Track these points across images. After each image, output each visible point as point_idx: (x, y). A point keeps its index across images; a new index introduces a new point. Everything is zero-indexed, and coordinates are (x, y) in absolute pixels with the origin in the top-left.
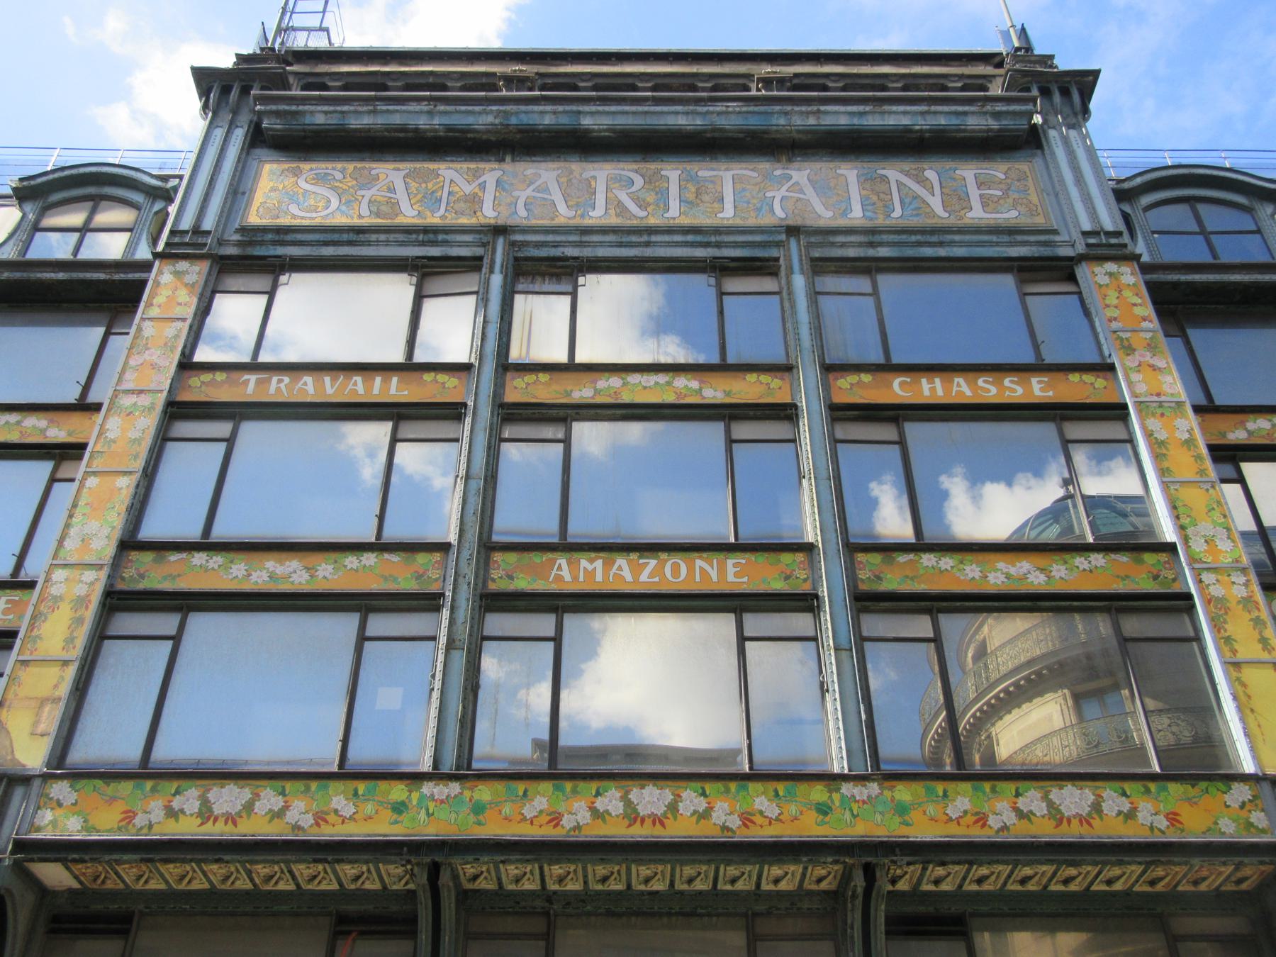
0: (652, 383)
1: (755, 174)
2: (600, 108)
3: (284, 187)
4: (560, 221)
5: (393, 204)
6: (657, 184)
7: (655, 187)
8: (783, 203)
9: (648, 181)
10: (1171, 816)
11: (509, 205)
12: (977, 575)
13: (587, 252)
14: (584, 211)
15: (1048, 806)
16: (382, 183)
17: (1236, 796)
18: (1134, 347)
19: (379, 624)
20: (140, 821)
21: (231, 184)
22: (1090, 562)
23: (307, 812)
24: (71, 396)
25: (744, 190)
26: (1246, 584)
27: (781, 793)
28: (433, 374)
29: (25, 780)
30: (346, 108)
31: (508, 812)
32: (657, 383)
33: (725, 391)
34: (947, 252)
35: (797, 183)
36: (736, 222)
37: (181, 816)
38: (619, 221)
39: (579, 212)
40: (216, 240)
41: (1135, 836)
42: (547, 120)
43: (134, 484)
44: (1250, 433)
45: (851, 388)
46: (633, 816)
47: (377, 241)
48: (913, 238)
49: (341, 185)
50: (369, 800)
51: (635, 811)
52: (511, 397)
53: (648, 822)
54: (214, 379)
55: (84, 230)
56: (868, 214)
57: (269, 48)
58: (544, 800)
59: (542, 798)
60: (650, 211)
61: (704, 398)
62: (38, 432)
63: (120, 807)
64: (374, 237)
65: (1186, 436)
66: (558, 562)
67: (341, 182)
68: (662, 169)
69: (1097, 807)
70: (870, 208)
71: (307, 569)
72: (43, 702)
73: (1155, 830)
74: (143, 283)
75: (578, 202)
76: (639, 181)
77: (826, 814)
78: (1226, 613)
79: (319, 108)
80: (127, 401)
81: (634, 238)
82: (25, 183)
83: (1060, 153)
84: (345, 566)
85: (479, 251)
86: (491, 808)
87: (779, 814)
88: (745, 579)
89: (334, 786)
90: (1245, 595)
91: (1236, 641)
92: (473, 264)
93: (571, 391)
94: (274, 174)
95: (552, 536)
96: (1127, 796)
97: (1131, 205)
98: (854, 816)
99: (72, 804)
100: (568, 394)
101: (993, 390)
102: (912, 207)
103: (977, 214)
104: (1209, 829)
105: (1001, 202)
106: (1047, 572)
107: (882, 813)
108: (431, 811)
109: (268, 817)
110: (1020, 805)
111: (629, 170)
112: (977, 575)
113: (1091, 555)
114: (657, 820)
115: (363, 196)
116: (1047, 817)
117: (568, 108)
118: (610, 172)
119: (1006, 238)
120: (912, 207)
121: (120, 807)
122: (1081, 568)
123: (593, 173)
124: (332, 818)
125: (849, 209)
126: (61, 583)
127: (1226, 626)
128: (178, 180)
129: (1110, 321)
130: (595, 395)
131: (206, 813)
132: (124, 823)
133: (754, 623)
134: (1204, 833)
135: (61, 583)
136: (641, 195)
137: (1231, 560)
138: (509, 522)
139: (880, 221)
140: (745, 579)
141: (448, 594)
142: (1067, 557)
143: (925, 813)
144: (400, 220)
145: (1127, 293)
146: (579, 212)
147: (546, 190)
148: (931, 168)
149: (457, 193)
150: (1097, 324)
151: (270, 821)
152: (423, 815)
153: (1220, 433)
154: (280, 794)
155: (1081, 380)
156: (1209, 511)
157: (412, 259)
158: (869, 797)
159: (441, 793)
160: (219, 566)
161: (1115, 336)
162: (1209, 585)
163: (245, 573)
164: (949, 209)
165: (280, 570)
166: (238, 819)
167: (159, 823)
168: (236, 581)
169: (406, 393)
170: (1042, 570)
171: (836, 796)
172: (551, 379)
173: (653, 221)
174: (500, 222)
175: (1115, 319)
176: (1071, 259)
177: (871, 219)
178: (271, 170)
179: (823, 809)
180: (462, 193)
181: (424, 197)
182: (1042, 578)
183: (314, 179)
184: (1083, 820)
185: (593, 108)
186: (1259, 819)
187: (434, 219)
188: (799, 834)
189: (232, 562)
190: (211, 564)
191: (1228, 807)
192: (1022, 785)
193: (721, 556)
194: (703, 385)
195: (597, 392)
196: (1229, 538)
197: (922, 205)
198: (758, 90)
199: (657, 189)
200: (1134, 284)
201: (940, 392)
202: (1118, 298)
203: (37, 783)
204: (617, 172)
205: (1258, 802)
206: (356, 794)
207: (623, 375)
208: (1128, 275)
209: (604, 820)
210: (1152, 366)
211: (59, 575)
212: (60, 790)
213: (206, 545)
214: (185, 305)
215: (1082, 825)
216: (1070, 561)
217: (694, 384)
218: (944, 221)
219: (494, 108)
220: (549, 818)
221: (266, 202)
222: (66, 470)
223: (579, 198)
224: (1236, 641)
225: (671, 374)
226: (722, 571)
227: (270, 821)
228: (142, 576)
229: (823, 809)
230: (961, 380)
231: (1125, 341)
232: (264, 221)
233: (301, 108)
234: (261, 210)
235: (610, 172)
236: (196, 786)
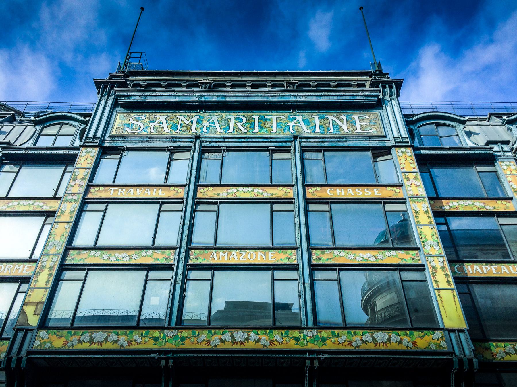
0: (247, 191)
1: (284, 117)
2: (232, 94)
4: (218, 134)
5: (162, 128)
8: (293, 127)
9: (248, 120)
10: (414, 343)
11: (201, 128)
12: (352, 258)
13: (227, 145)
15: (372, 339)
17: (436, 336)
18: (410, 178)
19: (153, 275)
20: (69, 344)
21: (107, 121)
22: (391, 254)
23: (125, 341)
24: (51, 195)
25: (280, 123)
26: (443, 262)
27: (283, 334)
28: (173, 188)
29: (32, 330)
30: (146, 94)
31: (192, 340)
32: (248, 191)
33: (271, 194)
34: (348, 144)
35: (298, 120)
37: (83, 343)
39: (224, 131)
40: (101, 141)
41: (401, 350)
42: (215, 99)
43: (71, 227)
44: (450, 207)
45: (313, 193)
46: (234, 341)
47: (156, 141)
48: (337, 140)
49: (144, 121)
50: (146, 336)
51: (235, 340)
52: (199, 195)
53: (239, 343)
54: (99, 190)
55: (57, 135)
56: (322, 131)
57: (121, 71)
58: (205, 336)
59: (204, 335)
61: (264, 196)
62: (40, 207)
63: (63, 339)
64: (155, 140)
65: (426, 210)
66: (213, 253)
67: (144, 120)
68: (253, 116)
69: (389, 340)
70: (322, 129)
72: (38, 303)
73: (409, 348)
74: (76, 155)
76: (245, 120)
77: (298, 341)
78: (436, 272)
79: (137, 94)
80: (70, 197)
81: (242, 140)
82: (37, 119)
83: (389, 108)
84: (142, 255)
85: (190, 144)
86: (187, 339)
87: (283, 341)
88: (275, 259)
89: (135, 332)
90: (443, 266)
91: (439, 282)
92: (187, 149)
93: (220, 193)
94: (122, 117)
95: (212, 244)
96: (400, 336)
97: (414, 126)
98: (308, 342)
99: (47, 339)
100: (218, 194)
101: (361, 193)
102: (336, 129)
103: (359, 131)
104: (426, 347)
106: (376, 257)
107: (317, 341)
108: (167, 340)
109: (112, 343)
110: (363, 338)
111: (241, 116)
112: (352, 258)
113: (391, 251)
114: (242, 343)
116: (372, 343)
117: (222, 94)
118: (235, 116)
119: (368, 140)
120: (336, 129)
121: (63, 339)
122: (388, 256)
123: (229, 117)
124: (134, 343)
125: (315, 129)
126: (45, 262)
127: (436, 276)
128: (89, 118)
129: (402, 169)
130: (227, 195)
131: (91, 342)
132: (64, 345)
133: (278, 274)
134: (425, 349)
135: (45, 262)
136: (245, 124)
137: (438, 253)
138: (197, 239)
139: (326, 134)
140: (275, 259)
141: (176, 264)
142: (383, 251)
143: (331, 341)
144: (164, 134)
145: (409, 159)
146: (224, 131)
147: (213, 123)
149: (183, 124)
150: (398, 170)
151: (113, 344)
152: (164, 342)
153: (440, 207)
154: (117, 335)
156: (432, 236)
157: (168, 148)
158: (313, 335)
159: (170, 334)
160: (99, 255)
161: (403, 174)
162: (431, 262)
163: (108, 258)
164: (349, 129)
165: (120, 257)
166: (102, 344)
167: (76, 345)
168: (105, 260)
169: (164, 194)
170: (375, 256)
171: (302, 335)
172: (213, 189)
173: (249, 134)
174: (198, 134)
175: (404, 168)
176: (390, 147)
177: (322, 133)
178: (121, 116)
182: (374, 259)
184: (385, 344)
185: (230, 94)
186: (443, 344)
187: (175, 134)
188: (289, 348)
189: (103, 254)
190: (97, 255)
191: (433, 340)
192: (364, 331)
193: (267, 251)
194: (264, 192)
195: (228, 194)
196: (438, 246)
198: (287, 87)
199: (251, 123)
200: (411, 156)
201: (343, 194)
203: (36, 331)
204: (238, 116)
205: (444, 338)
206: (142, 335)
207: (237, 188)
208: (409, 152)
209: (224, 343)
210: (416, 185)
211: (44, 258)
212: (43, 333)
213: (95, 248)
214: (90, 163)
215: (384, 346)
216: (384, 253)
217: (261, 191)
219: (197, 94)
220: (206, 342)
222: (50, 220)
223: (224, 126)
224: (439, 282)
225: (253, 187)
226: (267, 256)
227: (113, 344)
228: (73, 259)
229: (297, 339)
230: (350, 190)
233: (131, 94)
234: (117, 129)
235: (235, 116)
236: (89, 332)
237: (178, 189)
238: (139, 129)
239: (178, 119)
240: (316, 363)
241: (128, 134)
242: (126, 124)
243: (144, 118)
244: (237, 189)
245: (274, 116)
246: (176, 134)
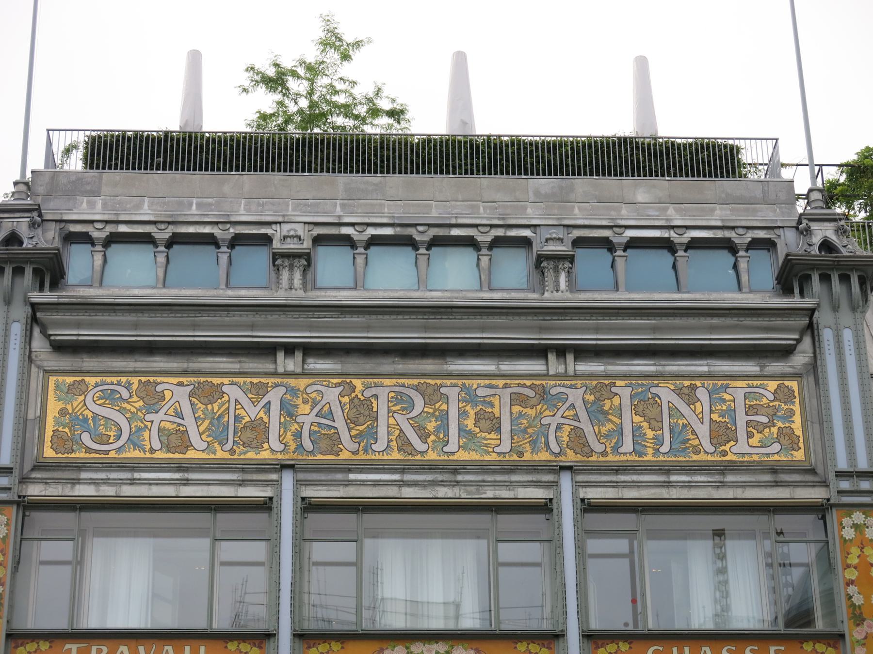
1: (531, 393)
3: (73, 410)
4: (345, 455)
6: (437, 405)
7: (435, 410)
14: (367, 443)
16: (167, 407)
36: (512, 459)
38: (402, 458)
49: (128, 407)
56: (637, 447)
60: (430, 444)
67: (128, 403)
68: (441, 386)
75: (361, 432)
85: (268, 492)
105: (767, 430)
115: (152, 422)
120: (681, 439)
123: (374, 391)
146: (362, 444)
148: (703, 386)
149: (242, 418)
155: (814, 650)
173: (432, 456)
175: (851, 582)
180: (247, 419)
181: (210, 423)
183: (101, 398)
197: (691, 437)
202: (859, 556)
204: (397, 389)
218: (710, 458)
221: (57, 429)
225: (450, 643)
231: (857, 609)
232: (60, 455)
237: (249, 646)
238: (118, 437)
239: (226, 398)
241: (88, 455)
242: (77, 417)
243: (125, 394)
244: (407, 648)
245: (505, 386)
246: (227, 456)
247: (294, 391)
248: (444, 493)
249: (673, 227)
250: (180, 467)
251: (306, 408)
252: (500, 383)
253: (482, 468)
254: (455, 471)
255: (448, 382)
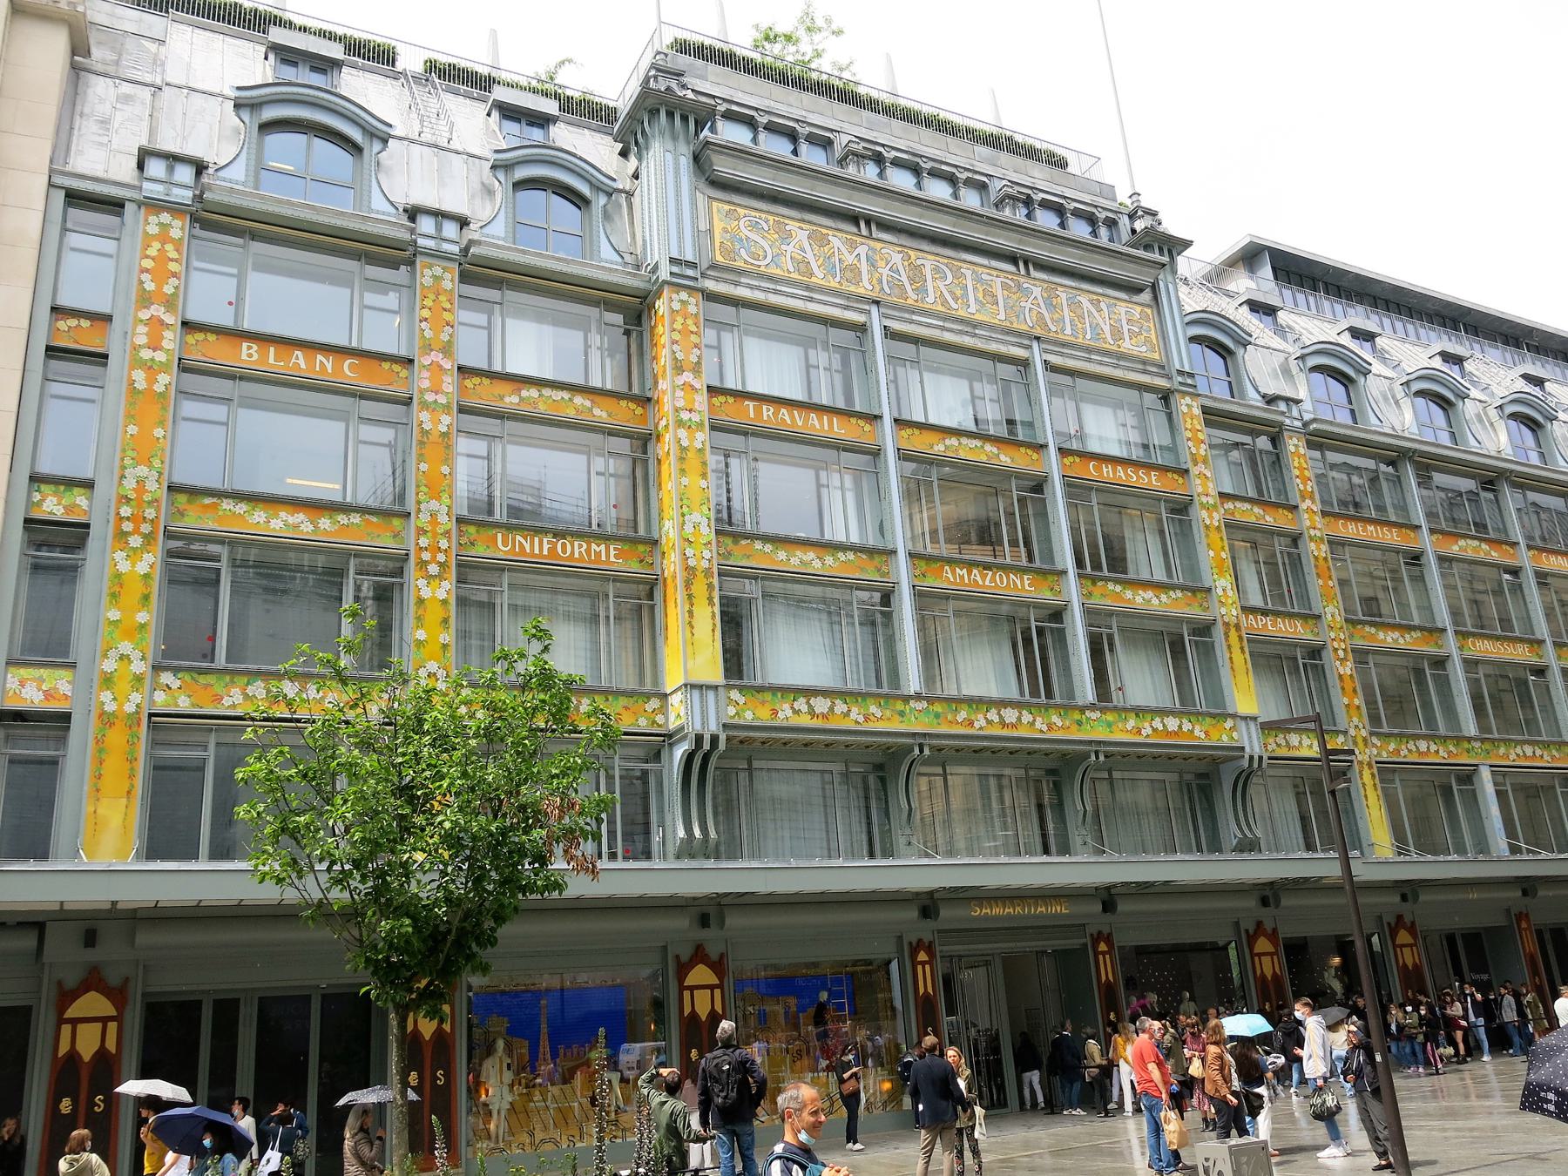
4: (910, 301)
46: (1003, 724)
71: (820, 559)
76: (950, 278)
121: (768, 707)
123: (922, 261)
173: (962, 313)
179: (1079, 723)
240: (1102, 758)
247: (874, 250)
248: (967, 341)
249: (1065, 197)
250: (808, 288)
251: (883, 264)
252: (995, 273)
253: (991, 327)
254: (975, 327)
255: (965, 266)
